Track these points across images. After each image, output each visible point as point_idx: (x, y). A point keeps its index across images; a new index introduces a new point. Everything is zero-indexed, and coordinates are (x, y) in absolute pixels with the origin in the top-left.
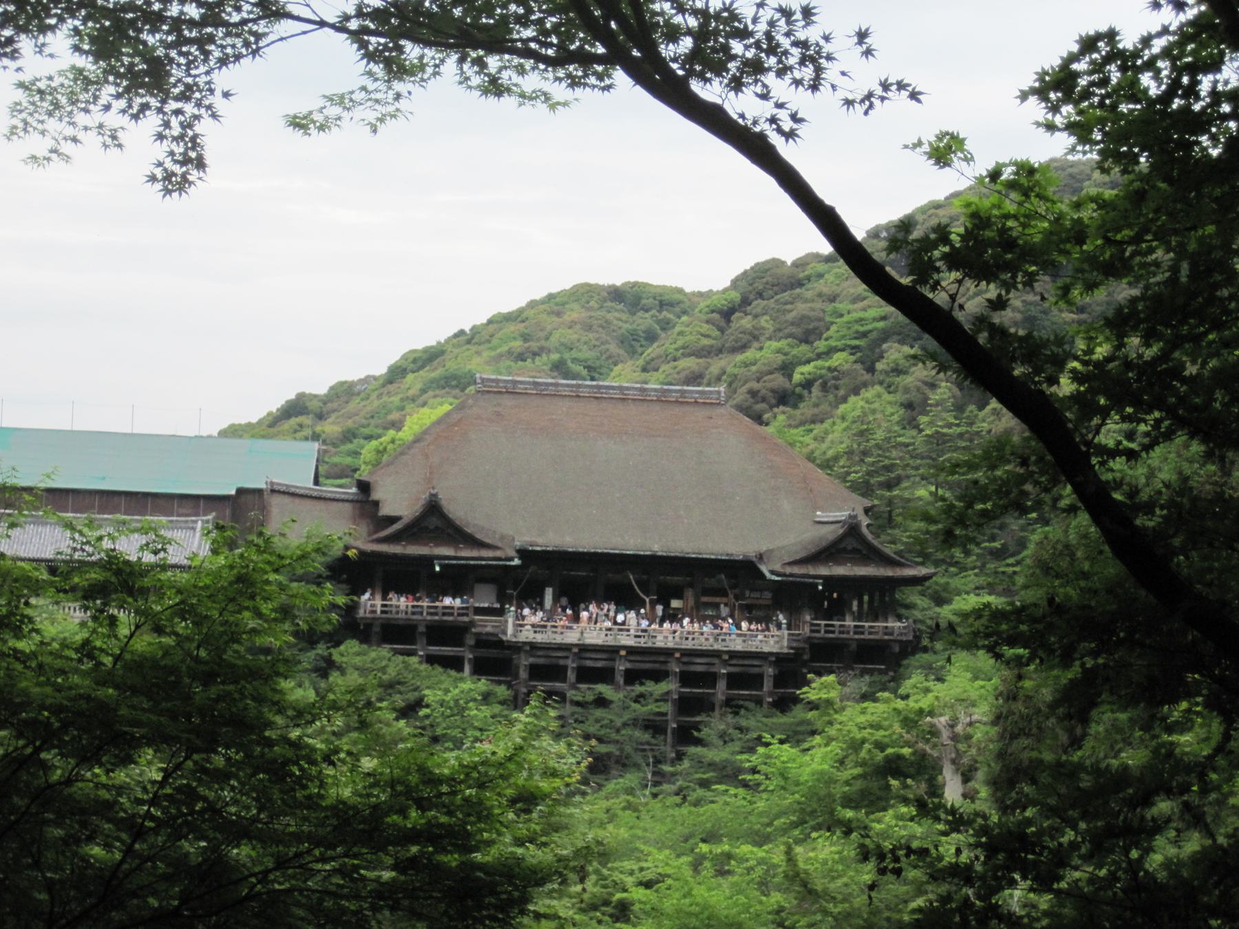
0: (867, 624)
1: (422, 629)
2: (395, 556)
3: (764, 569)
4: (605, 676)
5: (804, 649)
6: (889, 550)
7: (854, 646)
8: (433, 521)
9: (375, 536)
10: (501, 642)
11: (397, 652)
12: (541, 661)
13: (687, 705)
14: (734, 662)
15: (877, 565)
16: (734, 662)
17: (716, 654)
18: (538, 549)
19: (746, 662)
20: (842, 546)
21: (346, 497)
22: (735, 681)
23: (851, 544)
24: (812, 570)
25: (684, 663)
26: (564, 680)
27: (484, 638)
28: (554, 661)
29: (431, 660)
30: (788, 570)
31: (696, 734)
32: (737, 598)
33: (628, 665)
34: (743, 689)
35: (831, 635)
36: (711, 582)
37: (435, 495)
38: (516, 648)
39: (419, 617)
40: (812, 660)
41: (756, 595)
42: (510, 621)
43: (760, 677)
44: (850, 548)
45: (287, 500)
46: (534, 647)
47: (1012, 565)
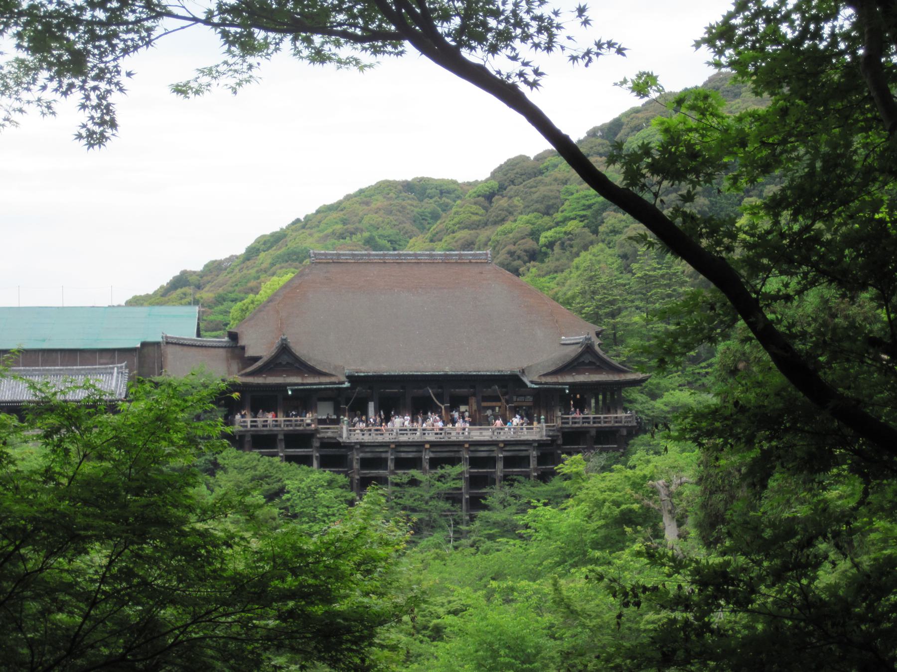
0: (602, 416)
1: (281, 437)
2: (258, 386)
3: (526, 380)
4: (414, 463)
6: (615, 361)
7: (593, 433)
8: (285, 358)
9: (243, 372)
10: (339, 443)
11: (263, 454)
12: (369, 455)
13: (475, 481)
14: (507, 448)
15: (608, 373)
16: (507, 448)
17: (494, 443)
18: (362, 374)
19: (517, 448)
20: (582, 360)
21: (221, 344)
22: (509, 462)
23: (588, 358)
24: (560, 379)
25: (472, 451)
26: (386, 469)
27: (326, 441)
28: (378, 455)
29: (289, 459)
30: (544, 380)
31: (483, 501)
32: (507, 402)
33: (432, 455)
35: (577, 425)
36: (488, 392)
37: (285, 340)
38: (350, 447)
39: (278, 429)
40: (564, 444)
41: (522, 398)
42: (345, 427)
43: (527, 458)
44: (587, 361)
45: (178, 348)
46: (362, 445)
47: (705, 368)
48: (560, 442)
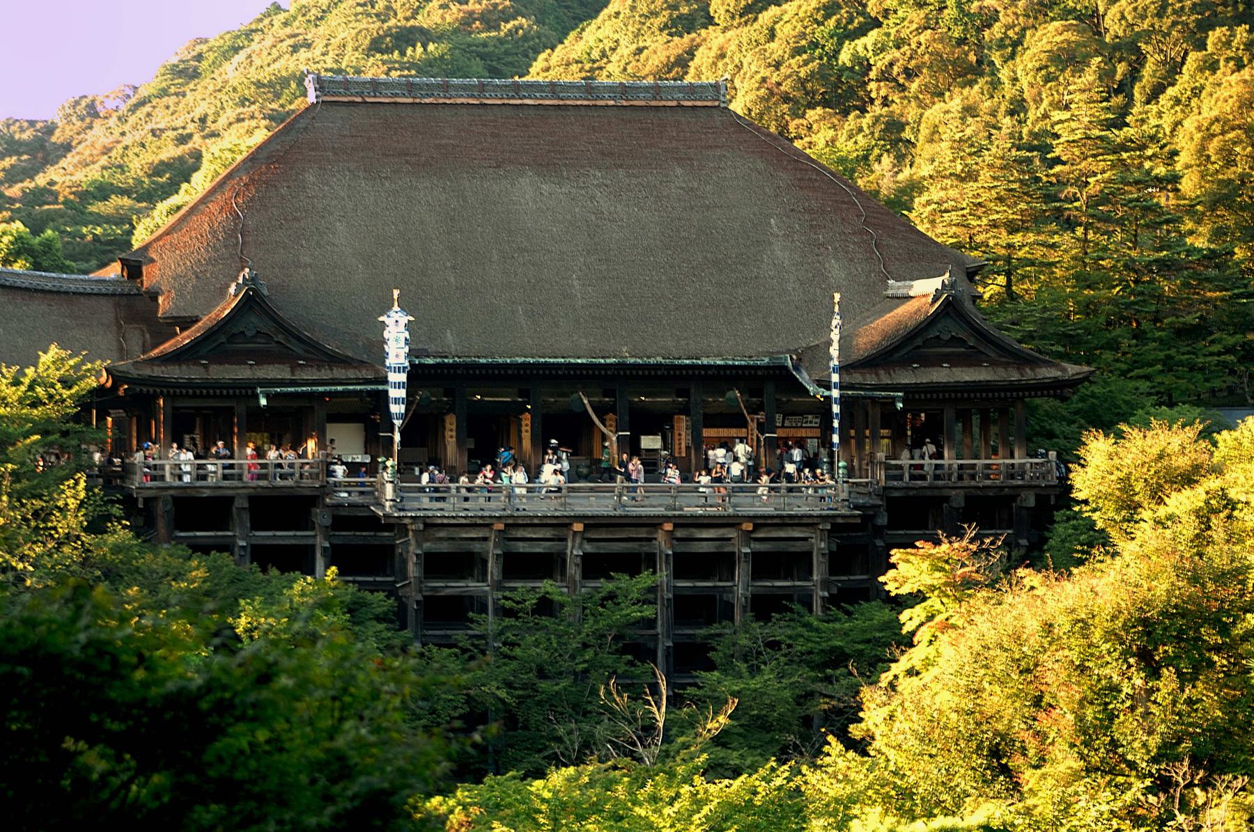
4: (548, 565)
5: (873, 507)
9: (154, 353)
12: (444, 547)
13: (688, 609)
15: (993, 364)
17: (732, 522)
18: (430, 361)
19: (782, 534)
20: (933, 333)
25: (679, 540)
27: (343, 513)
32: (762, 428)
33: (589, 548)
34: (778, 578)
39: (235, 483)
40: (892, 525)
43: (808, 555)
44: (946, 337)
46: (429, 525)
47: (1219, 354)
48: (883, 520)
